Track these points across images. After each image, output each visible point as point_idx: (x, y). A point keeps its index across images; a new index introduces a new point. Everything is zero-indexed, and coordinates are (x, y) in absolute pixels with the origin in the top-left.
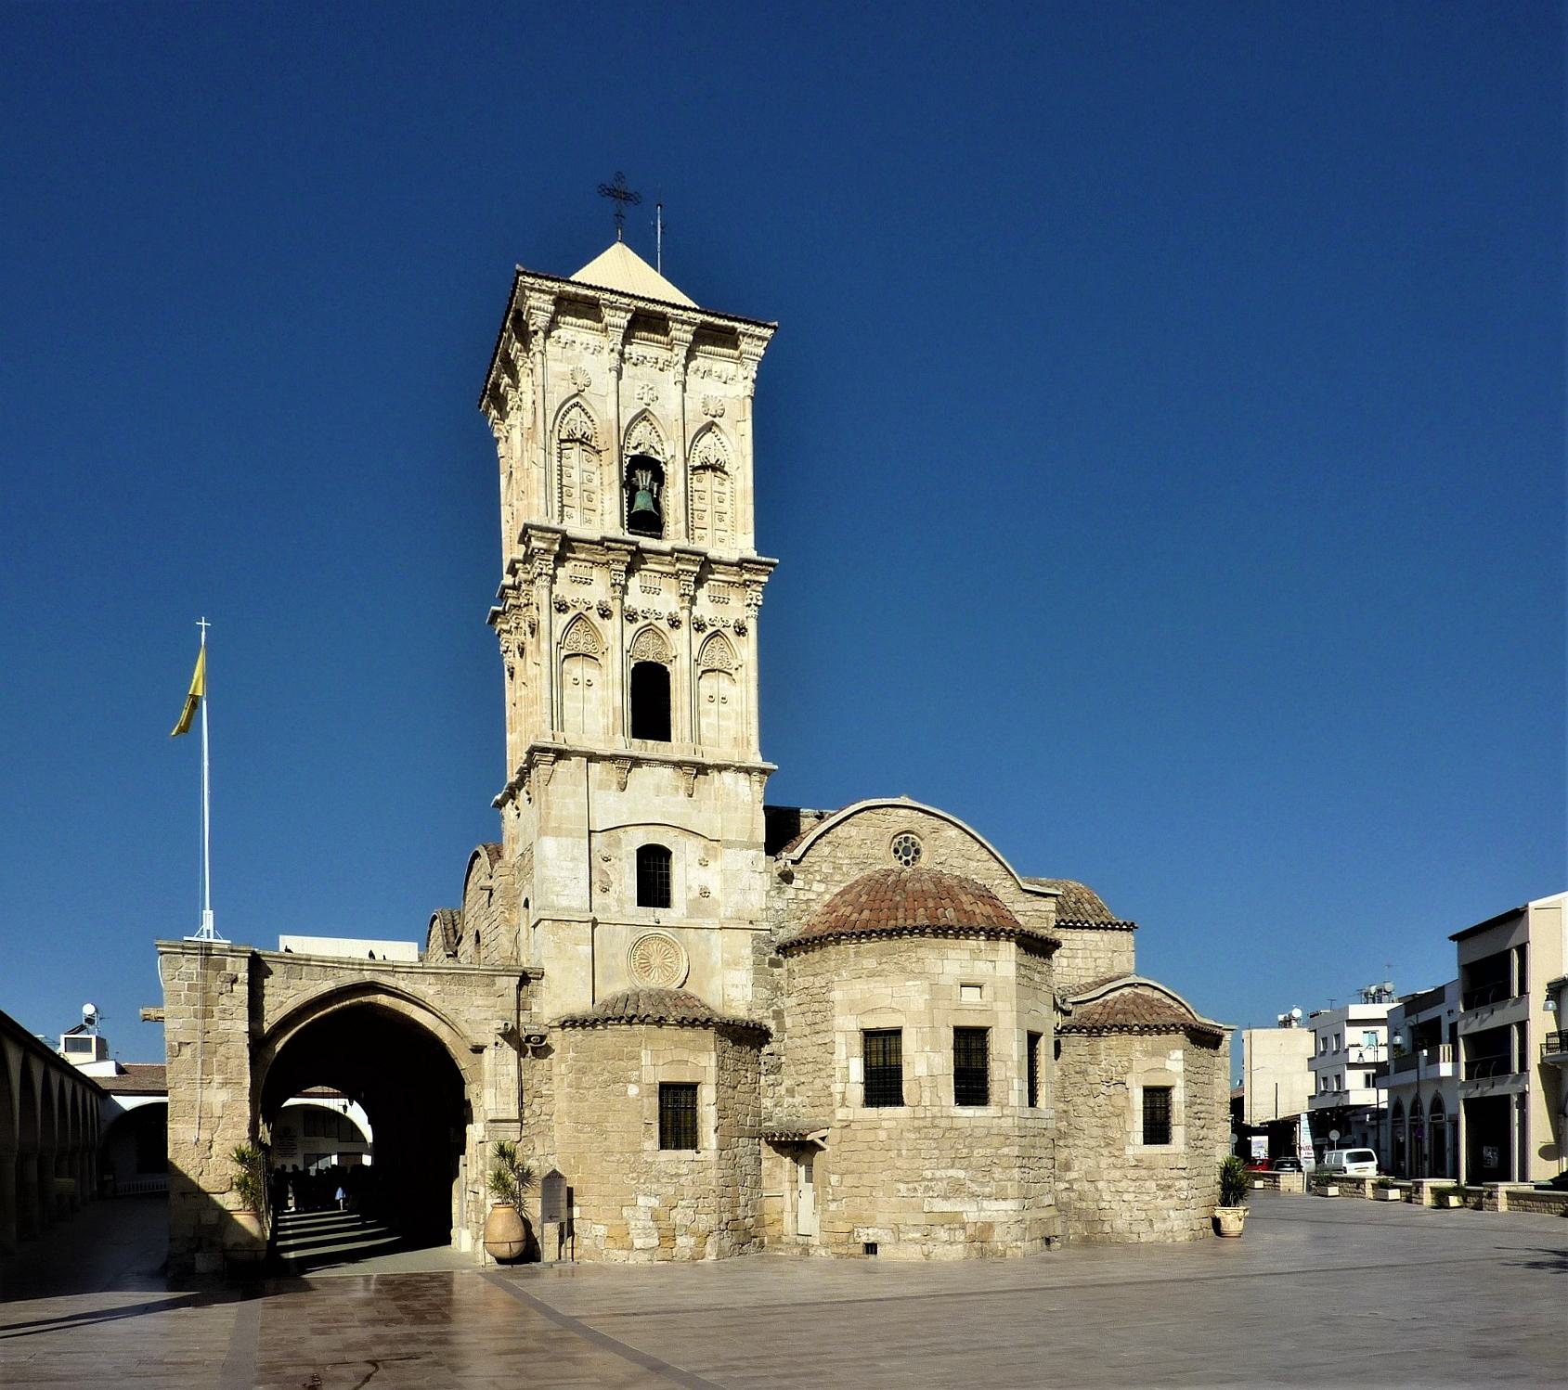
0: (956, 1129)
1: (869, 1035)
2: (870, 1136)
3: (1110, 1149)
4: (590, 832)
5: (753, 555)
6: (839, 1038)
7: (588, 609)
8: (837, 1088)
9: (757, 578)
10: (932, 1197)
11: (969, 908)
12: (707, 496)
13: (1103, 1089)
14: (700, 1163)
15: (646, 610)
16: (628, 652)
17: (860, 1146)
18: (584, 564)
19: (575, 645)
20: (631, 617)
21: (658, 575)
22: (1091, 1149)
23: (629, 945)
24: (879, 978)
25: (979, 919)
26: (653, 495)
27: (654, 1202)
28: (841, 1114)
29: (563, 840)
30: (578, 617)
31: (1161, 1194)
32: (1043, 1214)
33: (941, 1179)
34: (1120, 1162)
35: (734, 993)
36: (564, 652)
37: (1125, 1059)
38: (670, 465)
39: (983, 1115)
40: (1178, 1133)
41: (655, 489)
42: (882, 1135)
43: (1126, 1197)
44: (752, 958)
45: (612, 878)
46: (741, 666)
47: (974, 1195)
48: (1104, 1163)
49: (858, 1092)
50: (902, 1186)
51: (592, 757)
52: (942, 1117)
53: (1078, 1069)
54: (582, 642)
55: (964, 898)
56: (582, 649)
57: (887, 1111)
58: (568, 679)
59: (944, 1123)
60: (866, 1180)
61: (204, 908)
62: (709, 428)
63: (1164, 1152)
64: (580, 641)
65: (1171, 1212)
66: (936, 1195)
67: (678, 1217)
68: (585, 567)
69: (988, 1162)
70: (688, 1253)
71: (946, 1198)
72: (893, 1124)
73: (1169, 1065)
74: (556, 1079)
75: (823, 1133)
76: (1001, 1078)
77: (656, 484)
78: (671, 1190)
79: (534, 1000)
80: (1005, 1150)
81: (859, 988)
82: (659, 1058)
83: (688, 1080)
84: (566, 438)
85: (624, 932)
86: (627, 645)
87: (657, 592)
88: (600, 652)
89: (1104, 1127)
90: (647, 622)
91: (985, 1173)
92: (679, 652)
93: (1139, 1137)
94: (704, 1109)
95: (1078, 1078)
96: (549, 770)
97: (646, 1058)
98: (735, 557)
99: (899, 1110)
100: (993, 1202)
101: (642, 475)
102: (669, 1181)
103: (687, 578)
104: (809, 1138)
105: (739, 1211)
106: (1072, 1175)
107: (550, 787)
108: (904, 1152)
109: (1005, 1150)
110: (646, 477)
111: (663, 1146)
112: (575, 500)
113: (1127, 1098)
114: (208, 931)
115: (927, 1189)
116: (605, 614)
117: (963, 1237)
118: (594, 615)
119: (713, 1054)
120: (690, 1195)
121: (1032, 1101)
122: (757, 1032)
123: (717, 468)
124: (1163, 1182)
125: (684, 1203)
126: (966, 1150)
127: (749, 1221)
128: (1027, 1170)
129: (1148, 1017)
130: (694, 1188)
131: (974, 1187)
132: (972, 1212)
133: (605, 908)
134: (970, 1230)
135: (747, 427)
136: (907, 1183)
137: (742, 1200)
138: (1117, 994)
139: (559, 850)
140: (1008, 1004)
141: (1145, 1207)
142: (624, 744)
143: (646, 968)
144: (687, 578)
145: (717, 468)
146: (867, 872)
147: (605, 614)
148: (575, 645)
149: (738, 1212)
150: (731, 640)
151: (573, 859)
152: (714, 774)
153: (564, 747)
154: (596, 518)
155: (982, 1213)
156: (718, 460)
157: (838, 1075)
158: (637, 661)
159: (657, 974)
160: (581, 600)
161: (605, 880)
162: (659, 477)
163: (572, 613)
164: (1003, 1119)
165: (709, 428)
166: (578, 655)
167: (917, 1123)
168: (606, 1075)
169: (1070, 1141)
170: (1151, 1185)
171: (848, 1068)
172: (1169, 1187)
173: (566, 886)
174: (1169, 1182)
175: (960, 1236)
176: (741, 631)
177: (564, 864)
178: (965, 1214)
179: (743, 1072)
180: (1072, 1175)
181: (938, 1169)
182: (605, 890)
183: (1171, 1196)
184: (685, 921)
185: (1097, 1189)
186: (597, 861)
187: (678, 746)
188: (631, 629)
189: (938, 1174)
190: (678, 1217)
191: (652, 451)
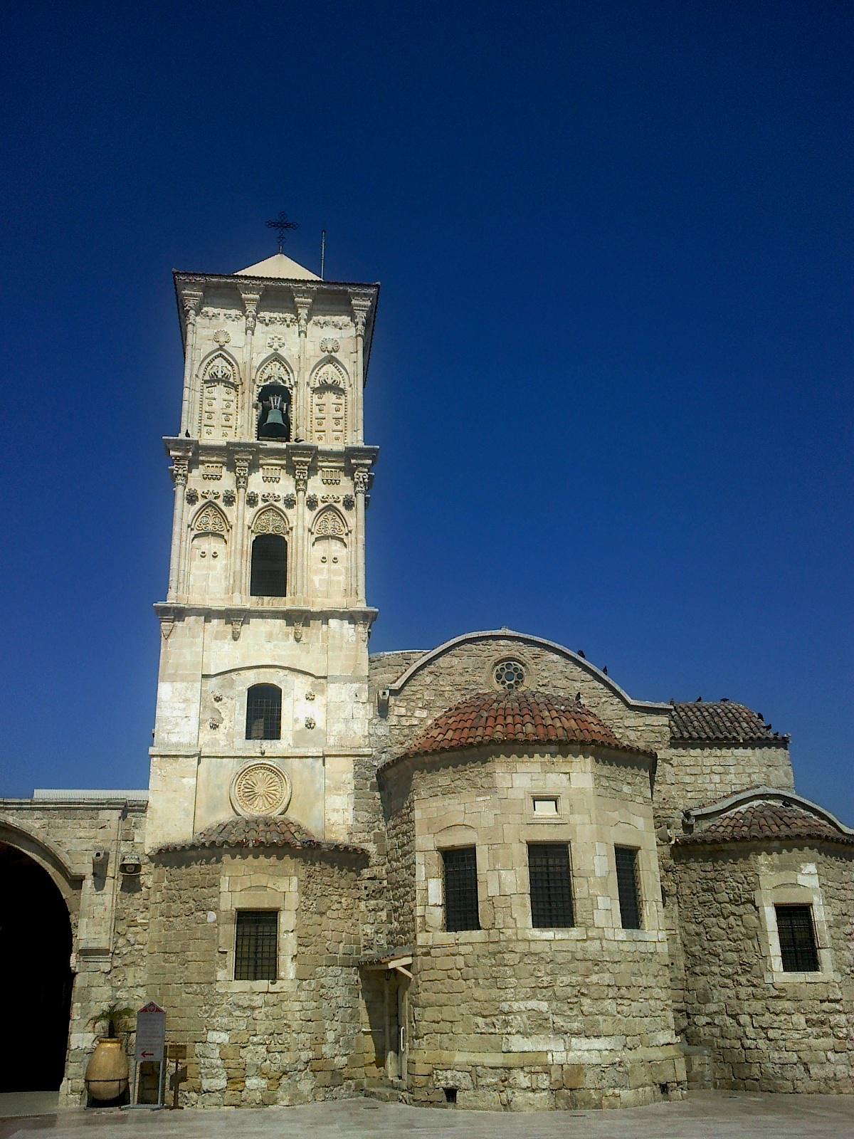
0: (536, 954)
2: (448, 962)
3: (748, 976)
5: (361, 445)
6: (419, 858)
8: (419, 911)
9: (362, 462)
10: (509, 1034)
13: (732, 908)
14: (276, 995)
15: (266, 495)
16: (249, 528)
17: (440, 975)
18: (215, 465)
19: (204, 526)
20: (252, 501)
21: (278, 468)
22: (728, 977)
24: (453, 795)
25: (560, 732)
26: (282, 411)
27: (224, 1037)
28: (422, 938)
29: (178, 685)
30: (210, 504)
31: (815, 1030)
32: (657, 1054)
33: (520, 1012)
34: (759, 991)
35: (335, 818)
36: (195, 532)
37: (750, 874)
38: (294, 389)
39: (567, 937)
40: (825, 956)
41: (285, 408)
42: (460, 961)
43: (771, 1034)
44: (353, 783)
45: (223, 715)
46: (350, 532)
47: (559, 1032)
48: (743, 992)
49: (438, 915)
50: (480, 1020)
51: (208, 615)
52: (518, 940)
53: (705, 887)
54: (211, 523)
57: (464, 935)
59: (521, 947)
60: (446, 1013)
63: (809, 980)
65: (829, 1053)
66: (514, 1031)
67: (247, 1055)
68: (216, 467)
69: (575, 992)
70: (258, 1096)
71: (525, 1034)
72: (468, 949)
73: (802, 880)
74: (152, 907)
75: (408, 961)
76: (583, 896)
77: (285, 404)
78: (242, 1025)
79: (137, 831)
80: (594, 978)
81: (436, 804)
82: (236, 884)
83: (266, 906)
84: (208, 378)
85: (231, 765)
86: (247, 522)
87: (277, 480)
88: (226, 530)
89: (738, 951)
90: (267, 503)
91: (571, 1006)
93: (777, 964)
94: (281, 936)
95: (708, 897)
96: (170, 626)
97: (224, 886)
99: (476, 933)
100: (584, 1040)
101: (274, 399)
102: (241, 1014)
103: (302, 467)
104: (391, 965)
105: (326, 1050)
106: (712, 1007)
107: (169, 640)
108: (481, 981)
109: (594, 978)
110: (278, 400)
113: (758, 918)
115: (506, 1023)
117: (547, 1083)
119: (295, 879)
120: (263, 1030)
121: (631, 917)
122: (354, 856)
124: (814, 1017)
125: (255, 1039)
126: (549, 978)
127: (341, 1061)
128: (625, 1002)
129: (775, 828)
130: (267, 1022)
131: (560, 1021)
132: (557, 1052)
134: (556, 1074)
136: (484, 1017)
137: (331, 1036)
138: (743, 808)
139: (173, 693)
140: (587, 816)
141: (796, 1047)
142: (244, 600)
143: (250, 795)
144: (302, 467)
148: (204, 526)
149: (324, 1050)
150: (343, 513)
151: (186, 700)
155: (571, 1054)
156: (335, 381)
157: (418, 898)
158: (259, 534)
160: (211, 491)
161: (216, 717)
162: (287, 398)
163: (201, 502)
164: (589, 942)
165: (331, 360)
167: (492, 947)
168: (192, 904)
169: (707, 968)
170: (800, 1020)
171: (427, 889)
172: (823, 1023)
173: (177, 724)
174: (822, 1017)
175: (544, 1081)
177: (177, 705)
178: (550, 1054)
179: (335, 898)
180: (712, 1007)
181: (516, 1000)
182: (214, 727)
183: (825, 1035)
184: (290, 751)
185: (739, 1024)
188: (250, 513)
189: (516, 1006)
190: (247, 1055)
191: (280, 381)
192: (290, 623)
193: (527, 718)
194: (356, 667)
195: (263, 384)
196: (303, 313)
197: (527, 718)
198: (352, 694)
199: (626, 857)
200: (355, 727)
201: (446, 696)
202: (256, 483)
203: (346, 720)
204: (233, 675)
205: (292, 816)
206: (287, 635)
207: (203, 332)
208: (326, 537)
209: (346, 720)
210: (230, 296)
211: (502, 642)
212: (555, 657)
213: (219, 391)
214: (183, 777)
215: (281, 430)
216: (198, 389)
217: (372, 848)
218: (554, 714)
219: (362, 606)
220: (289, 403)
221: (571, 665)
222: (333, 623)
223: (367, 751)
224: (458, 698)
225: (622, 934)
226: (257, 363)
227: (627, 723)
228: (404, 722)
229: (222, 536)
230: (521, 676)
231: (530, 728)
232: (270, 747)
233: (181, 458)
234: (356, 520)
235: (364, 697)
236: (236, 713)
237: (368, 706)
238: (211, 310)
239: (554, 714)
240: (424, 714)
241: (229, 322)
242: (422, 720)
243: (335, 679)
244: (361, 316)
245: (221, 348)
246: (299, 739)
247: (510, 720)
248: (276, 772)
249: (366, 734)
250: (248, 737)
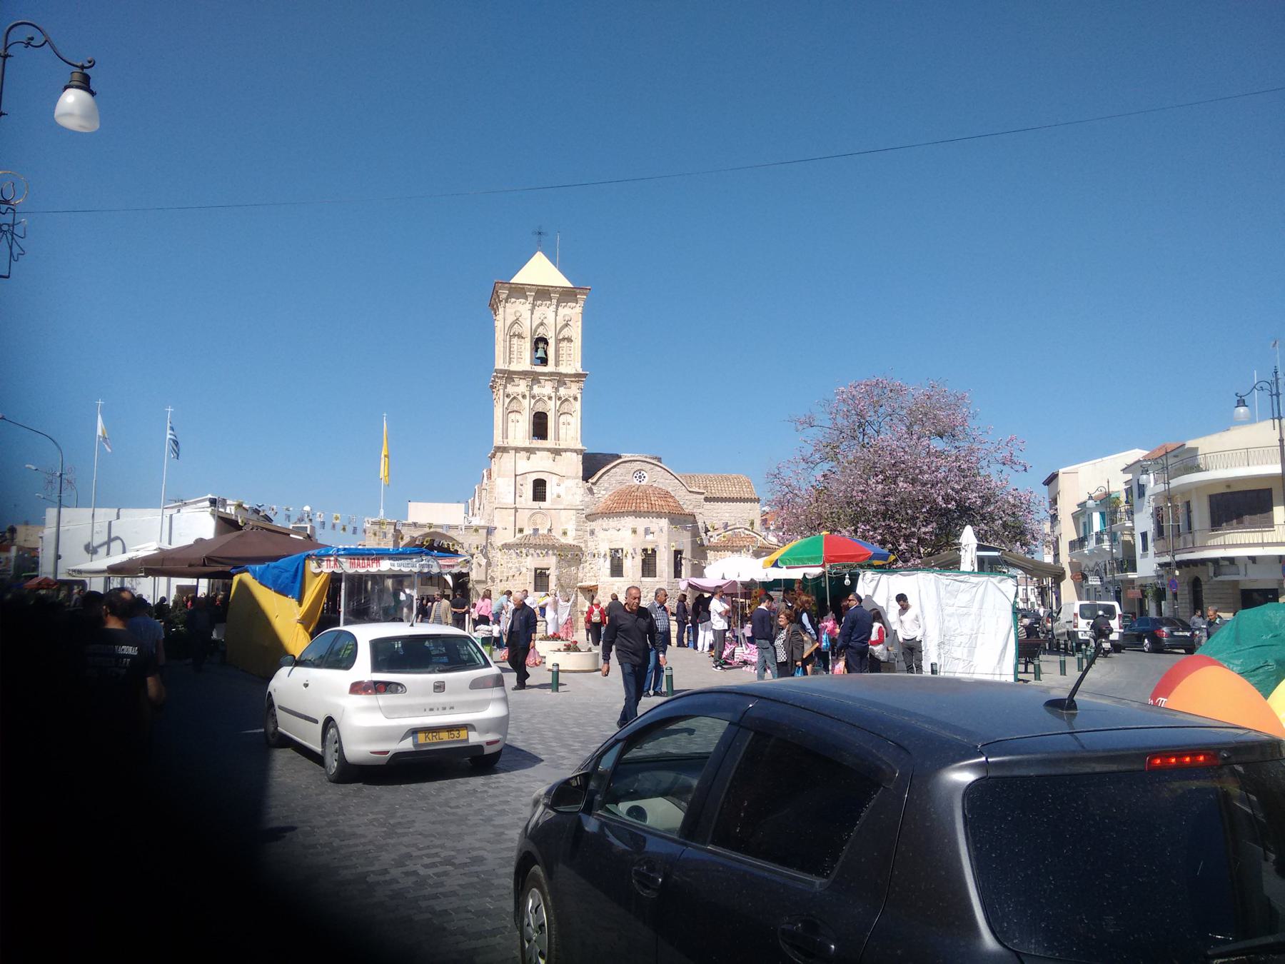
4: (516, 476)
7: (518, 395)
11: (653, 502)
12: (565, 349)
20: (534, 397)
23: (529, 516)
30: (514, 398)
45: (524, 491)
51: (517, 450)
55: (652, 499)
56: (515, 409)
58: (510, 420)
62: (567, 325)
64: (514, 406)
86: (531, 407)
92: (551, 408)
98: (573, 372)
111: (535, 591)
112: (515, 355)
116: (524, 397)
118: (520, 397)
121: (677, 574)
123: (569, 340)
133: (520, 503)
135: (580, 324)
145: (569, 340)
146: (623, 486)
147: (524, 397)
152: (563, 454)
153: (507, 445)
154: (522, 361)
165: (567, 325)
166: (514, 411)
176: (575, 399)
186: (518, 486)
187: (550, 443)
188: (533, 401)
192: (552, 453)
193: (645, 501)
194: (577, 472)
195: (536, 337)
196: (554, 301)
197: (645, 501)
199: (678, 553)
202: (536, 390)
203: (573, 495)
204: (527, 475)
207: (508, 310)
208: (564, 413)
209: (573, 495)
210: (519, 291)
211: (638, 463)
212: (660, 469)
213: (515, 340)
215: (544, 361)
216: (508, 340)
217: (582, 545)
218: (656, 499)
219: (579, 446)
221: (667, 473)
222: (569, 454)
223: (581, 507)
224: (619, 487)
225: (674, 580)
226: (533, 328)
227: (687, 498)
229: (520, 413)
230: (644, 477)
231: (645, 505)
232: (541, 504)
233: (503, 377)
234: (577, 406)
235: (580, 484)
236: (528, 491)
237: (582, 489)
238: (513, 300)
239: (656, 499)
240: (604, 492)
241: (521, 305)
242: (603, 495)
243: (568, 478)
244: (581, 303)
245: (517, 319)
246: (553, 501)
247: (638, 501)
248: (546, 515)
250: (533, 500)
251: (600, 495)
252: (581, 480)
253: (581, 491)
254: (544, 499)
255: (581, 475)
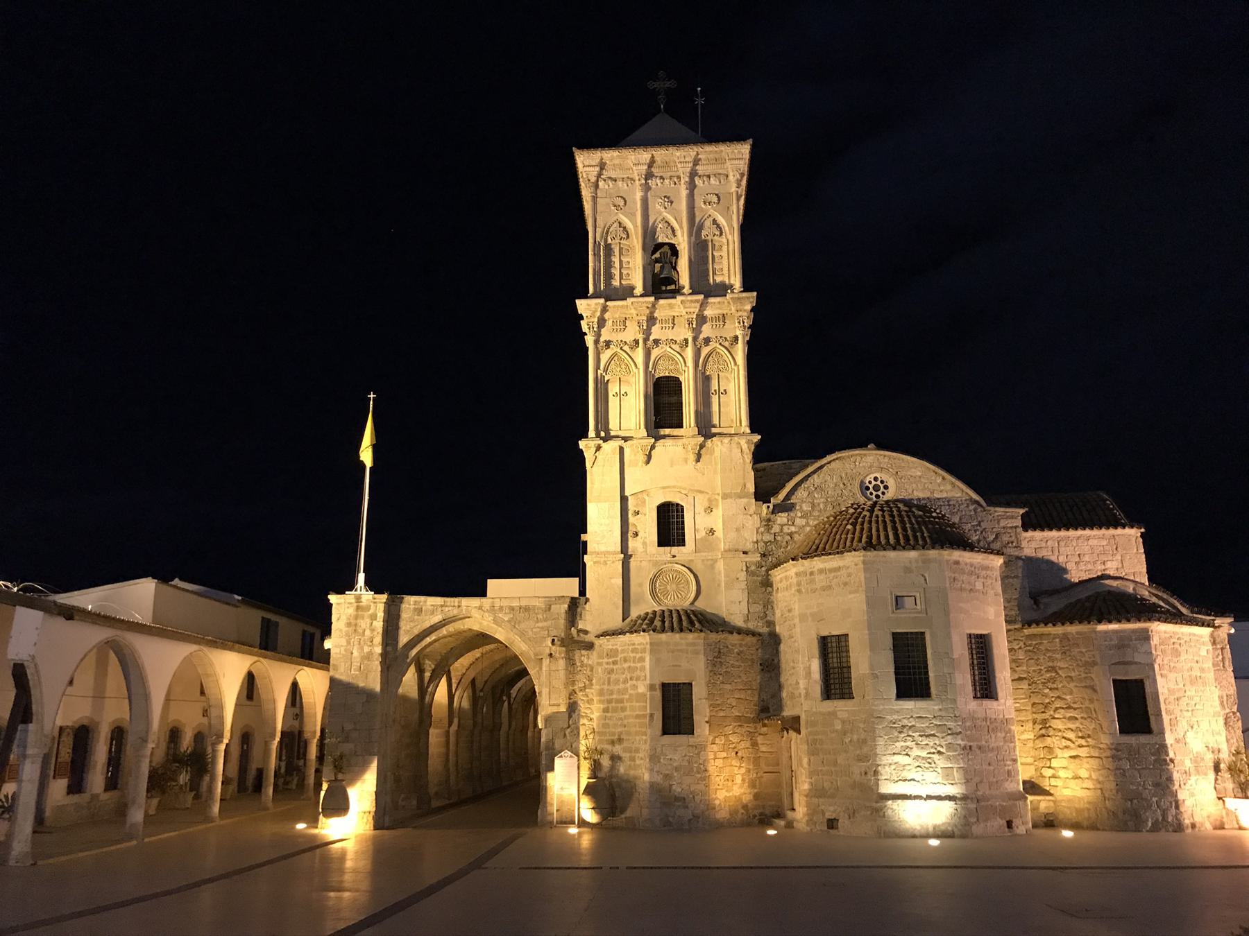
1: (824, 641)
4: (624, 499)
26: (672, 265)
49: (817, 690)
61: (359, 572)
114: (361, 587)
159: (679, 595)
171: (809, 668)
198: (743, 506)
200: (746, 535)
201: (822, 506)
203: (738, 530)
205: (701, 605)
206: (686, 460)
209: (738, 530)
214: (611, 578)
220: (677, 257)
228: (786, 529)
230: (886, 487)
235: (753, 508)
236: (647, 526)
237: (756, 518)
240: (803, 522)
249: (755, 540)
251: (793, 529)
252: (754, 500)
253: (753, 523)
254: (681, 542)
255: (751, 488)
